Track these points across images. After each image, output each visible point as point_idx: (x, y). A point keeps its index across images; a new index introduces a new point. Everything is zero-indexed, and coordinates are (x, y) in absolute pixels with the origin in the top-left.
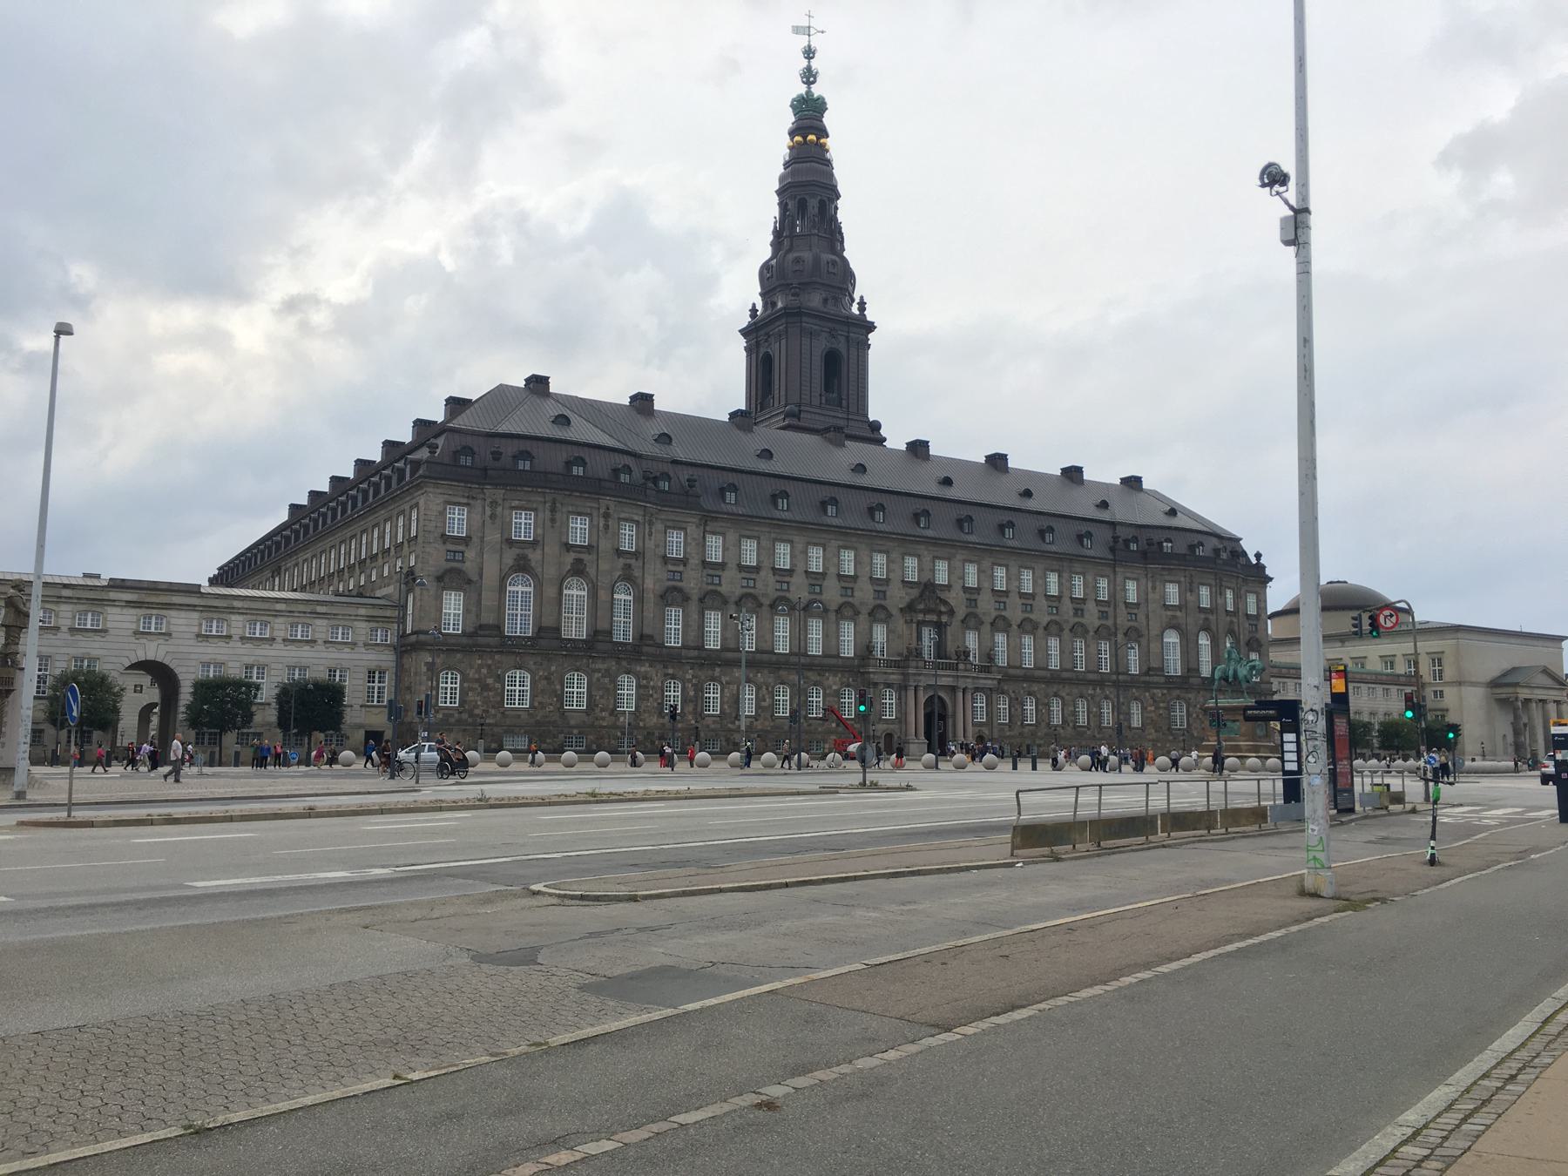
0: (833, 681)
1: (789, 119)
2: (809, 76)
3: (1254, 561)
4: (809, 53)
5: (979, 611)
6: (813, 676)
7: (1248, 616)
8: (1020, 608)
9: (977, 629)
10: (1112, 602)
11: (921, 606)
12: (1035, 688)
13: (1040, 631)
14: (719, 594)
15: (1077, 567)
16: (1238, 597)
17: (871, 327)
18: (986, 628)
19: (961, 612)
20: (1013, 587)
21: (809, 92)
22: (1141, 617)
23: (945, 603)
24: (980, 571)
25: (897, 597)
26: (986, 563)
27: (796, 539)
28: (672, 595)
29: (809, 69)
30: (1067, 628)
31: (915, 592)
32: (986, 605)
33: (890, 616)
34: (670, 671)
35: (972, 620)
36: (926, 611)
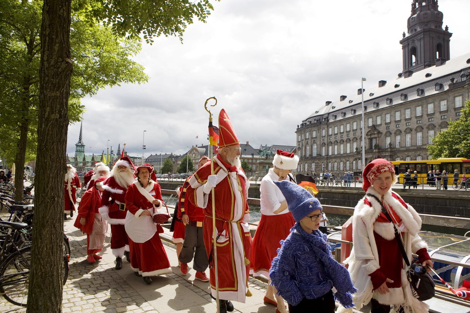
0: (351, 159)
5: (390, 130)
6: (347, 159)
8: (405, 125)
12: (410, 154)
13: (414, 132)
15: (430, 100)
18: (393, 135)
20: (393, 120)
24: (391, 116)
26: (393, 112)
27: (345, 123)
28: (324, 144)
30: (425, 127)
31: (370, 129)
32: (393, 128)
35: (389, 134)
36: (370, 135)
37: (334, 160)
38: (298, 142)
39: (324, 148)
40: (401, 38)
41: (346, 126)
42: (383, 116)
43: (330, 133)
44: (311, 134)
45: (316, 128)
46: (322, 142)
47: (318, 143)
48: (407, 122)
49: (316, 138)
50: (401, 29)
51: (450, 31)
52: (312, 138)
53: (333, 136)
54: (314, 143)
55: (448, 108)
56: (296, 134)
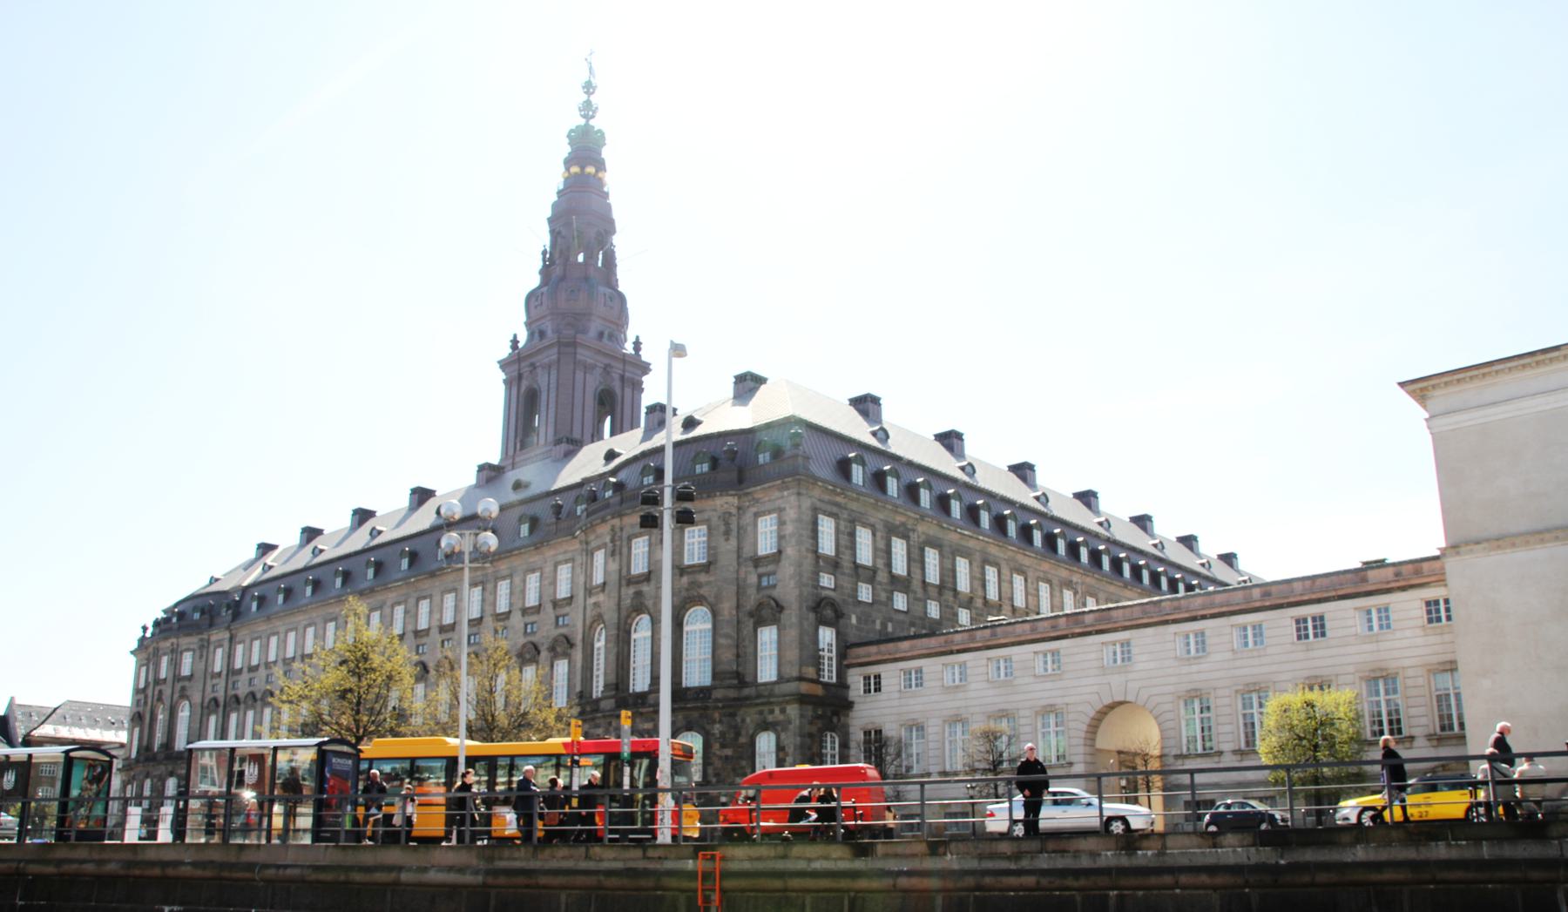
7: (757, 561)
21: (587, 125)
29: (588, 104)
38: (137, 691)
39: (213, 719)
40: (506, 351)
42: (387, 610)
43: (238, 664)
44: (175, 664)
45: (193, 640)
46: (209, 695)
47: (197, 698)
48: (444, 636)
49: (190, 678)
50: (509, 324)
51: (645, 356)
52: (177, 678)
53: (245, 676)
54: (184, 695)
55: (541, 597)
56: (133, 659)
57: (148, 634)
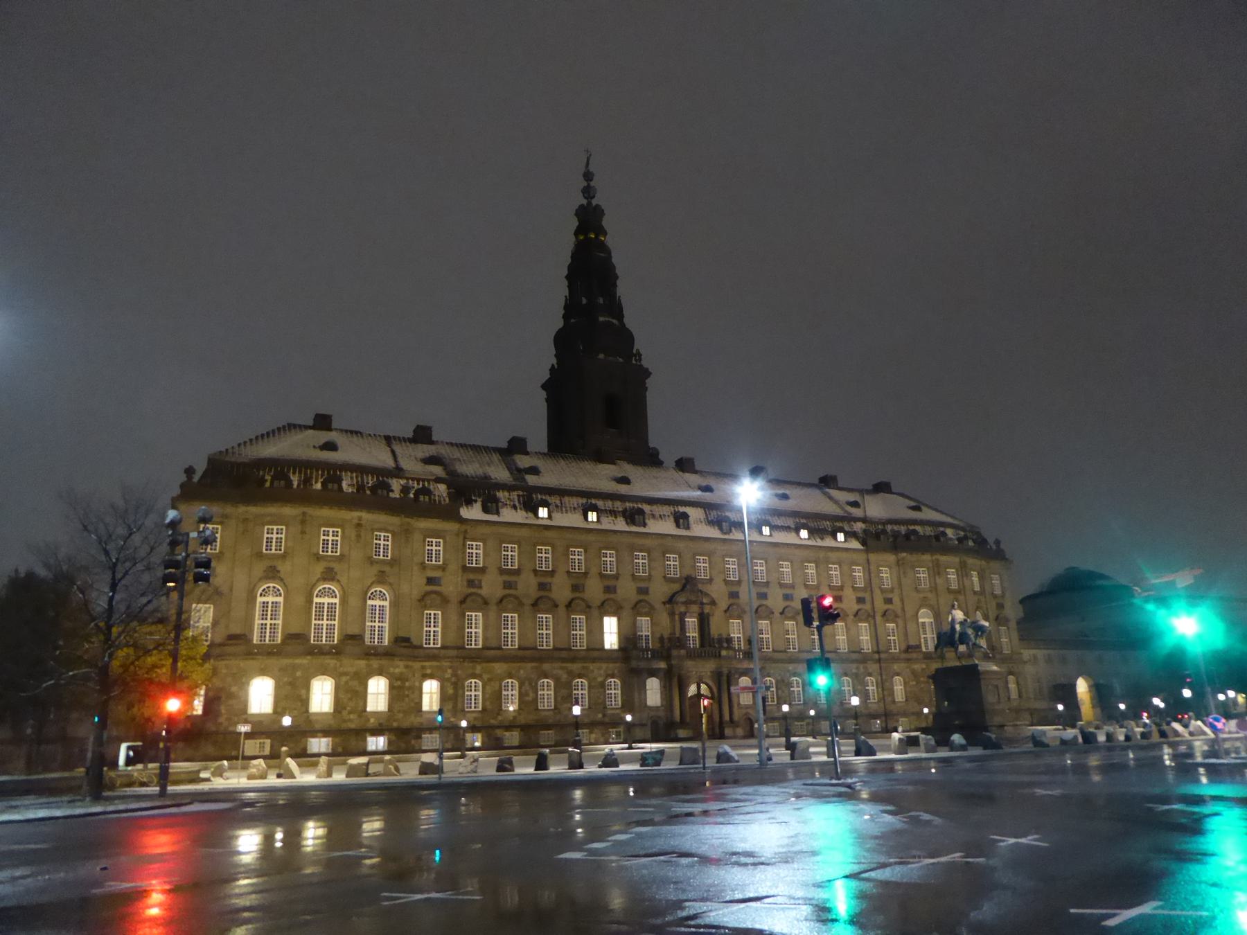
1: (574, 223)
2: (588, 192)
3: (994, 547)
4: (588, 176)
9: (739, 617)
10: (869, 586)
11: (683, 599)
14: (480, 595)
16: (982, 578)
17: (647, 373)
19: (723, 604)
22: (896, 600)
23: (707, 595)
25: (659, 591)
31: (677, 587)
33: (652, 608)
34: (429, 671)
37: (499, 668)
41: (566, 554)
57: (196, 478)
